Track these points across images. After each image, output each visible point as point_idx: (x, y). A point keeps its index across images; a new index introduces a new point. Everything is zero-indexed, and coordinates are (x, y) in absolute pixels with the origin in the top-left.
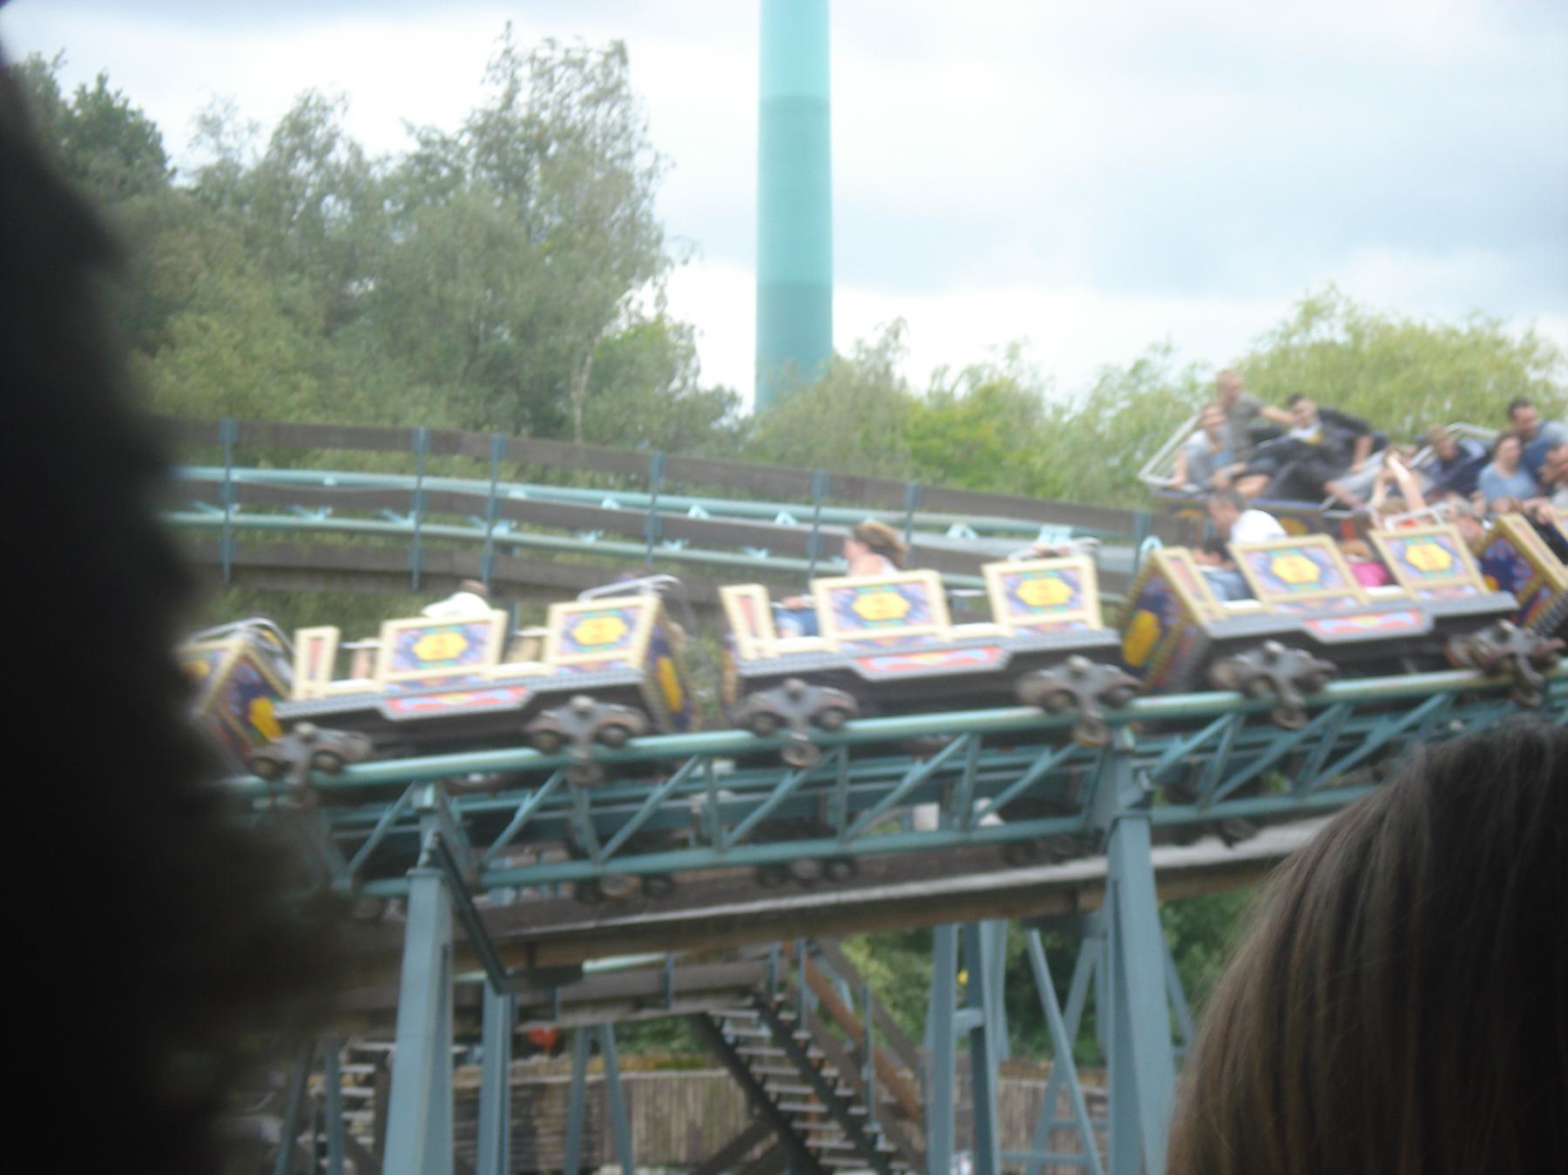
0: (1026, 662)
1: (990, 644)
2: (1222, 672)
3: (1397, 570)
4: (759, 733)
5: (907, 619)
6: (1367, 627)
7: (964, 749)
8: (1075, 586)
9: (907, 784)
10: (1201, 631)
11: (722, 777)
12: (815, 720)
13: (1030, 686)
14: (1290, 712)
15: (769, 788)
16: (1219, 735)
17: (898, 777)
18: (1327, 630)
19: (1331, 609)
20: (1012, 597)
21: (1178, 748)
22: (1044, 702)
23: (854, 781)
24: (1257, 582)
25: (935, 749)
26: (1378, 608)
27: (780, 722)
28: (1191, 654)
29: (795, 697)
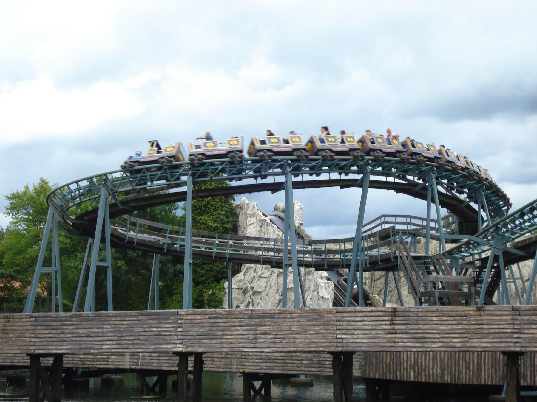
0: (295, 150)
1: (289, 147)
2: (320, 153)
3: (345, 141)
4: (232, 159)
5: (207, 143)
6: (340, 149)
7: (227, 164)
8: (292, 141)
9: (276, 166)
10: (369, 147)
11: (249, 164)
12: (199, 160)
13: (229, 156)
14: (329, 160)
15: (255, 166)
16: (319, 162)
17: (275, 165)
18: (334, 149)
19: (335, 146)
20: (292, 141)
21: (314, 163)
22: (298, 156)
23: (211, 169)
24: (375, 141)
25: (281, 161)
26: (342, 147)
27: (235, 157)
28: (315, 150)
29: (265, 152)
